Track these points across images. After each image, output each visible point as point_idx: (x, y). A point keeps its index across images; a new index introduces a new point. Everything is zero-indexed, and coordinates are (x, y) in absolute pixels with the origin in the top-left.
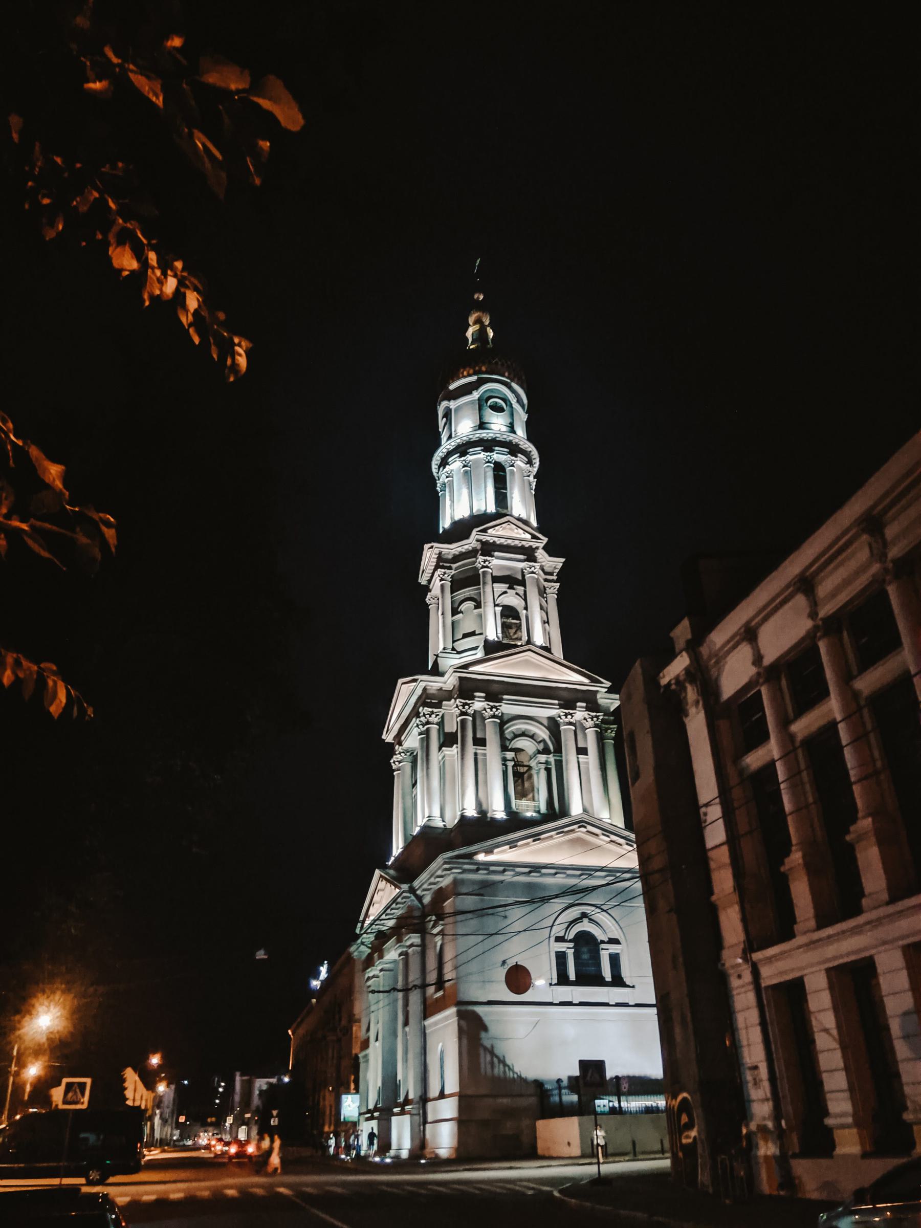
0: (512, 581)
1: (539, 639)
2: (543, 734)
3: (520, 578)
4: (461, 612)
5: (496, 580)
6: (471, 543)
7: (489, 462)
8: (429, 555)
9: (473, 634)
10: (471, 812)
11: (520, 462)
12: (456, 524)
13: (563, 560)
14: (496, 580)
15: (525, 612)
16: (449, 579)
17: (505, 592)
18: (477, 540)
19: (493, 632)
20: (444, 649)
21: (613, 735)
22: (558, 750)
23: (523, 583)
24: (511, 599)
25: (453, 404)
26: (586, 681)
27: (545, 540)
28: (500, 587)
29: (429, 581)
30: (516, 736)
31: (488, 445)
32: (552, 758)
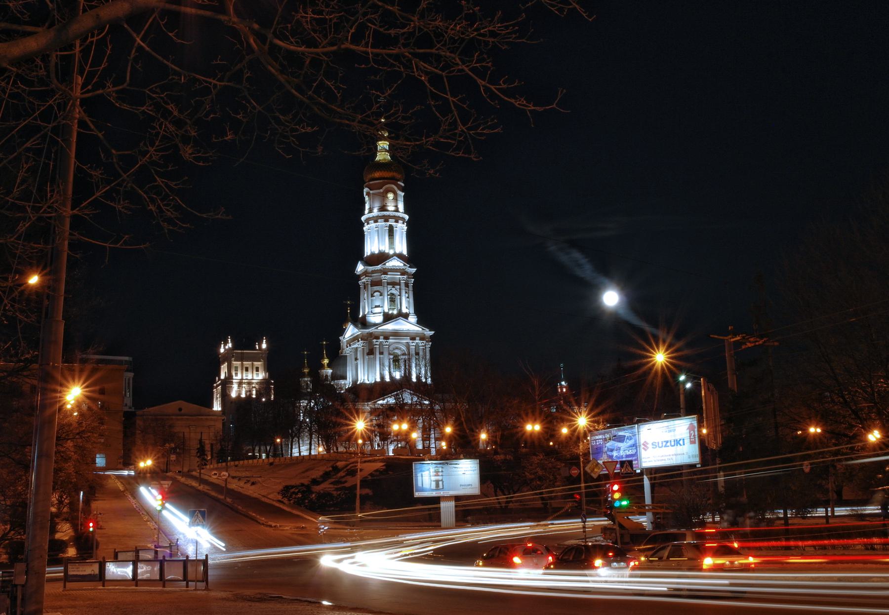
0: (393, 284)
2: (404, 348)
3: (398, 282)
4: (373, 296)
5: (389, 284)
10: (378, 380)
12: (373, 255)
13: (416, 269)
14: (389, 284)
15: (399, 297)
17: (391, 289)
23: (399, 284)
24: (394, 291)
25: (371, 192)
28: (390, 287)
30: (394, 349)
31: (386, 219)
32: (407, 357)
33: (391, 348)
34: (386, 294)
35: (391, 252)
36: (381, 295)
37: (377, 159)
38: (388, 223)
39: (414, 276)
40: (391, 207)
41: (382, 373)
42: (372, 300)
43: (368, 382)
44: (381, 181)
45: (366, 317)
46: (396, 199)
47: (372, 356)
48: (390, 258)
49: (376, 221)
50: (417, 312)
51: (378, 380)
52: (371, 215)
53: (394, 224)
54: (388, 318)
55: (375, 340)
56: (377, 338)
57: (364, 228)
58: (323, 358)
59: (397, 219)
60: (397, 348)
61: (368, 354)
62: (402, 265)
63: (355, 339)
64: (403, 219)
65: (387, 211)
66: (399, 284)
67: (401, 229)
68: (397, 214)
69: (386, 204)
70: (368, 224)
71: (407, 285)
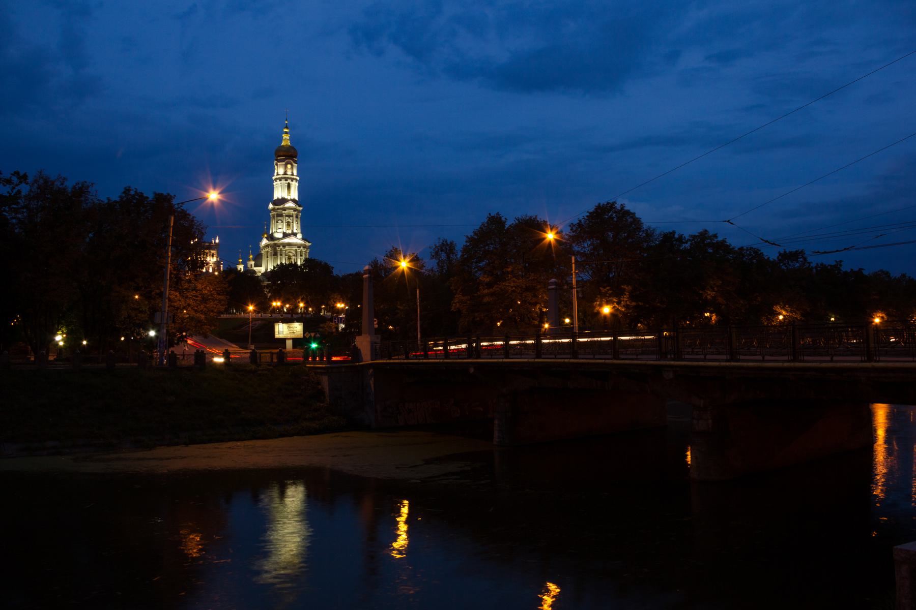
0: (289, 216)
2: (294, 252)
12: (278, 199)
14: (286, 216)
22: (296, 256)
23: (292, 216)
24: (289, 220)
25: (279, 163)
28: (287, 218)
31: (286, 179)
32: (295, 257)
33: (287, 252)
34: (285, 222)
35: (289, 198)
36: (282, 222)
37: (282, 144)
38: (287, 182)
40: (289, 173)
46: (292, 168)
49: (280, 180)
50: (302, 232)
52: (278, 176)
53: (291, 182)
54: (285, 235)
56: (279, 246)
57: (274, 184)
58: (250, 255)
59: (292, 180)
60: (290, 252)
61: (274, 255)
62: (294, 206)
63: (267, 246)
64: (296, 179)
65: (287, 175)
66: (292, 216)
67: (295, 185)
68: (292, 177)
70: (276, 181)
71: (297, 217)
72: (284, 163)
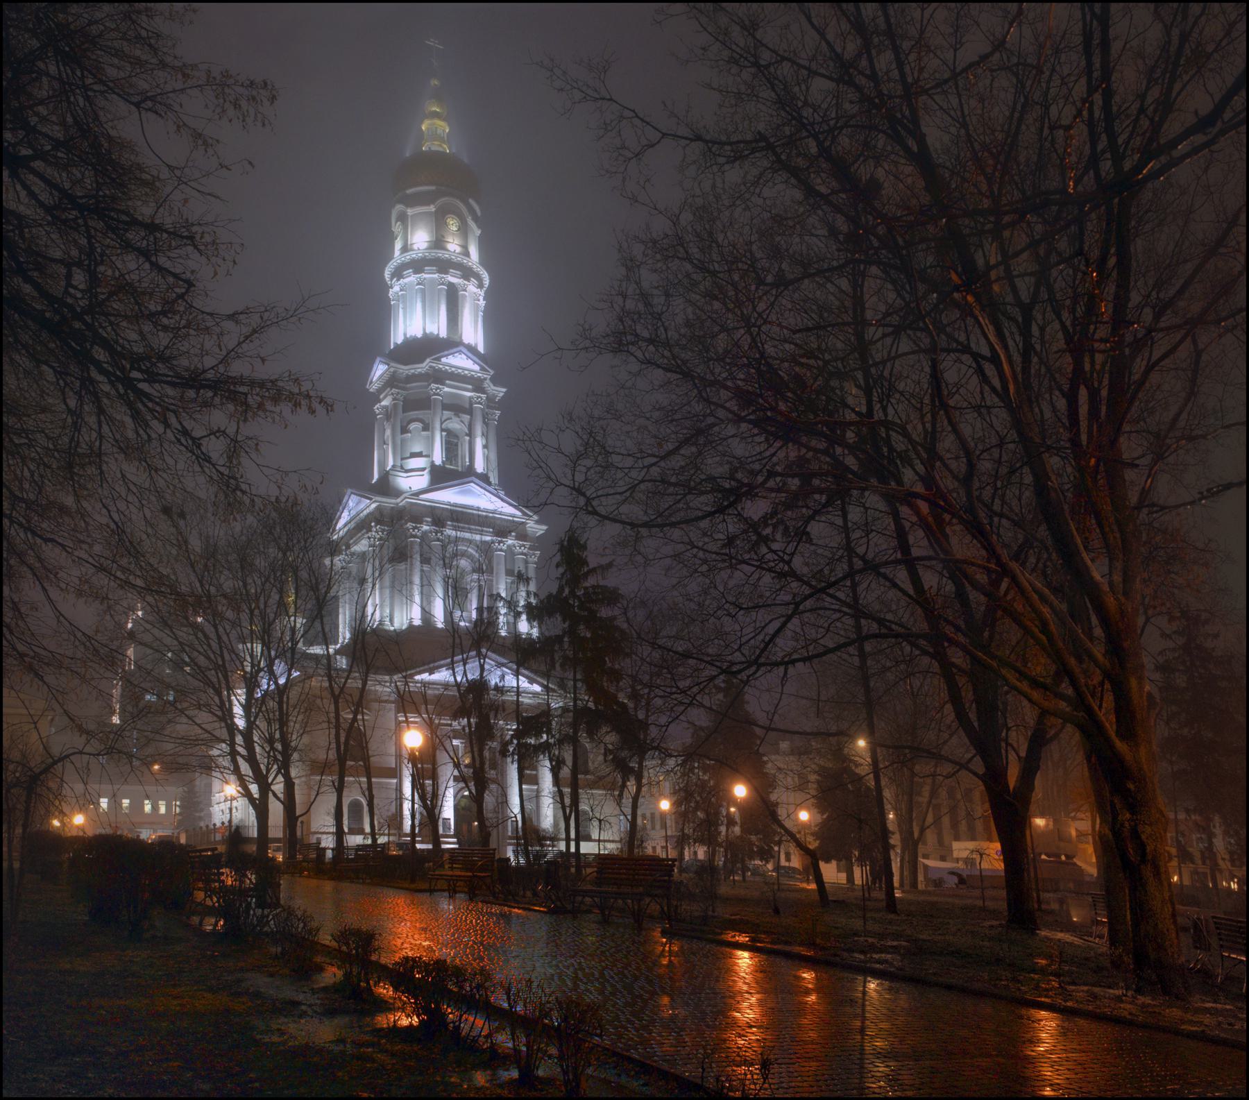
0: (457, 408)
1: (479, 466)
3: (467, 406)
6: (423, 367)
7: (443, 284)
8: (379, 370)
9: (419, 455)
10: (417, 622)
11: (472, 288)
13: (504, 390)
14: (446, 407)
15: (467, 438)
16: (402, 398)
18: (431, 367)
19: (438, 457)
20: (393, 466)
21: (536, 559)
22: (490, 571)
23: (470, 411)
24: (456, 425)
25: (410, 212)
26: (518, 513)
27: (492, 372)
28: (447, 414)
29: (380, 391)
31: (444, 266)
34: (437, 425)
39: (503, 404)
41: (427, 609)
42: (403, 441)
43: (392, 628)
44: (433, 188)
45: (391, 478)
47: (402, 566)
48: (452, 348)
51: (417, 622)
52: (408, 257)
54: (440, 477)
55: (409, 525)
56: (417, 519)
61: (392, 560)
62: (477, 368)
66: (470, 411)
67: (474, 296)
69: (443, 237)
72: (432, 208)
